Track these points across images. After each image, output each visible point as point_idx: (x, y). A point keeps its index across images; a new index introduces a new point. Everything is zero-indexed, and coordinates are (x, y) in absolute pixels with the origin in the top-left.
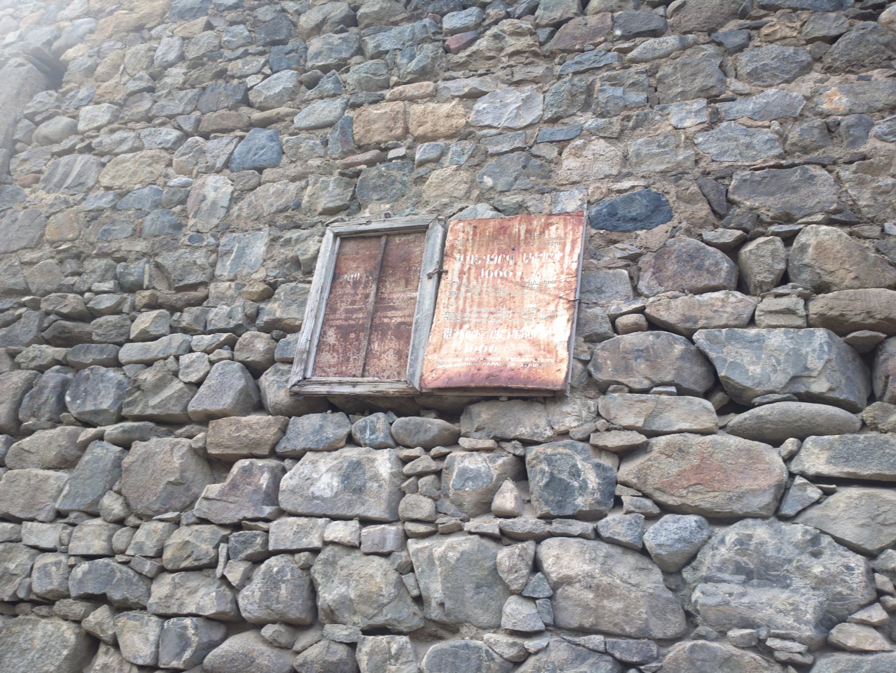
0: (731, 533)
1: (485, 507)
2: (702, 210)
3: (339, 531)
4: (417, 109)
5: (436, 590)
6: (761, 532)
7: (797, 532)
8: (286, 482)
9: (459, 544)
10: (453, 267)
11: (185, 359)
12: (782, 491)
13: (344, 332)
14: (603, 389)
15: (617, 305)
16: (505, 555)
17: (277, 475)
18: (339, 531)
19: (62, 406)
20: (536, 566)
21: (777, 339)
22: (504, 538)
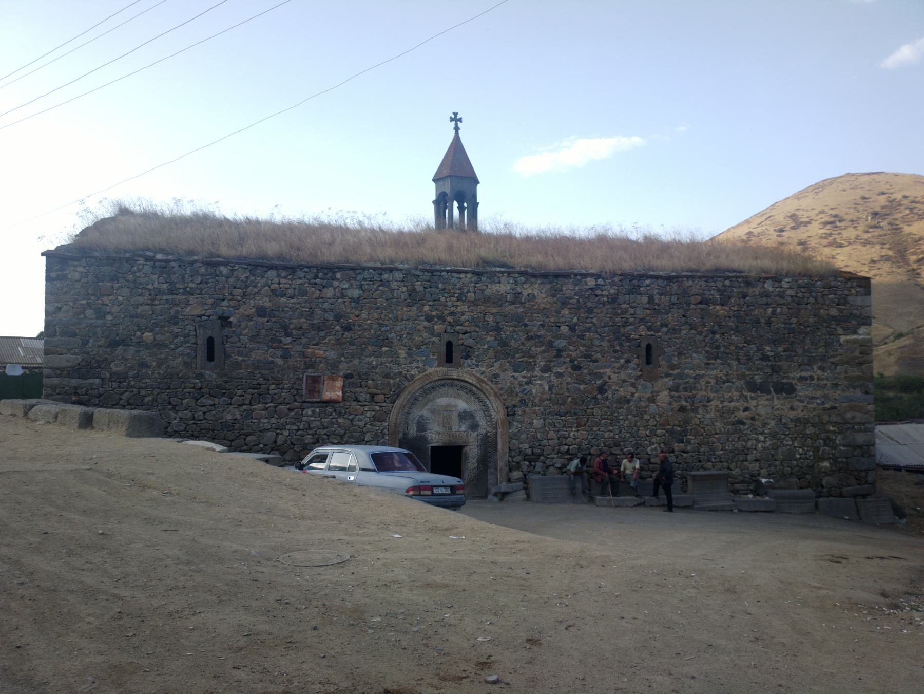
0: (357, 417)
1: (331, 415)
2: (357, 377)
3: (312, 419)
4: (316, 351)
5: (326, 424)
6: (360, 417)
7: (364, 416)
8: (304, 413)
9: (329, 419)
10: (325, 382)
11: (283, 394)
12: (363, 412)
13: (309, 391)
14: (345, 400)
15: (347, 390)
16: (334, 420)
17: (302, 412)
18: (312, 419)
19: (260, 401)
20: (337, 421)
21: (364, 395)
22: (334, 418)
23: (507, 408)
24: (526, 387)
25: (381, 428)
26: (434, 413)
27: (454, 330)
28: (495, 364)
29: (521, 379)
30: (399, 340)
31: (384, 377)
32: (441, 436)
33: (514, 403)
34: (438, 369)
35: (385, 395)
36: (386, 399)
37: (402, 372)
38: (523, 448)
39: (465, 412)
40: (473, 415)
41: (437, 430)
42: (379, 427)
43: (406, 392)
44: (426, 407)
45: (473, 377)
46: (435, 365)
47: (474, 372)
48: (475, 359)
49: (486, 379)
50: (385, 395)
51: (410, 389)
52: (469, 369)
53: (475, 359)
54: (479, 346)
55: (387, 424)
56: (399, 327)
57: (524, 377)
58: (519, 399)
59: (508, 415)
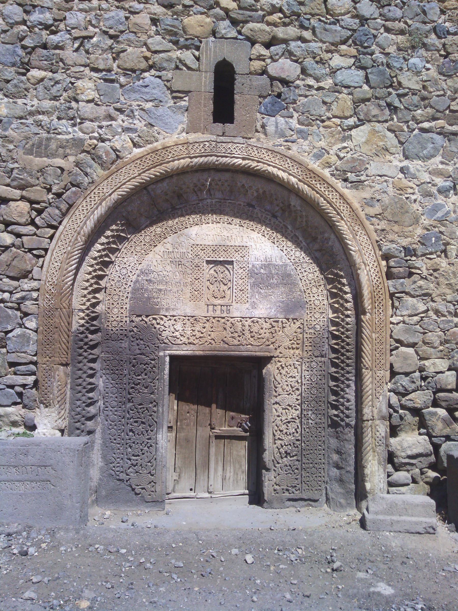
23: (386, 257)
24: (440, 200)
25: (18, 295)
26: (180, 264)
27: (240, 33)
28: (353, 132)
29: (426, 177)
30: (77, 50)
31: (29, 152)
32: (198, 327)
33: (405, 242)
34: (192, 137)
35: (31, 202)
36: (34, 213)
37: (82, 141)
38: (432, 370)
39: (268, 265)
40: (289, 275)
41: (189, 312)
42: (11, 293)
43: (94, 197)
44: (160, 248)
45: (288, 164)
46: (180, 127)
47: (294, 150)
48: (296, 115)
49: (326, 173)
50: (31, 202)
51: (106, 188)
52: (281, 141)
53: (296, 115)
54: (311, 82)
55: (35, 284)
56: (81, 16)
57: (438, 173)
58: (419, 231)
59: (390, 275)
